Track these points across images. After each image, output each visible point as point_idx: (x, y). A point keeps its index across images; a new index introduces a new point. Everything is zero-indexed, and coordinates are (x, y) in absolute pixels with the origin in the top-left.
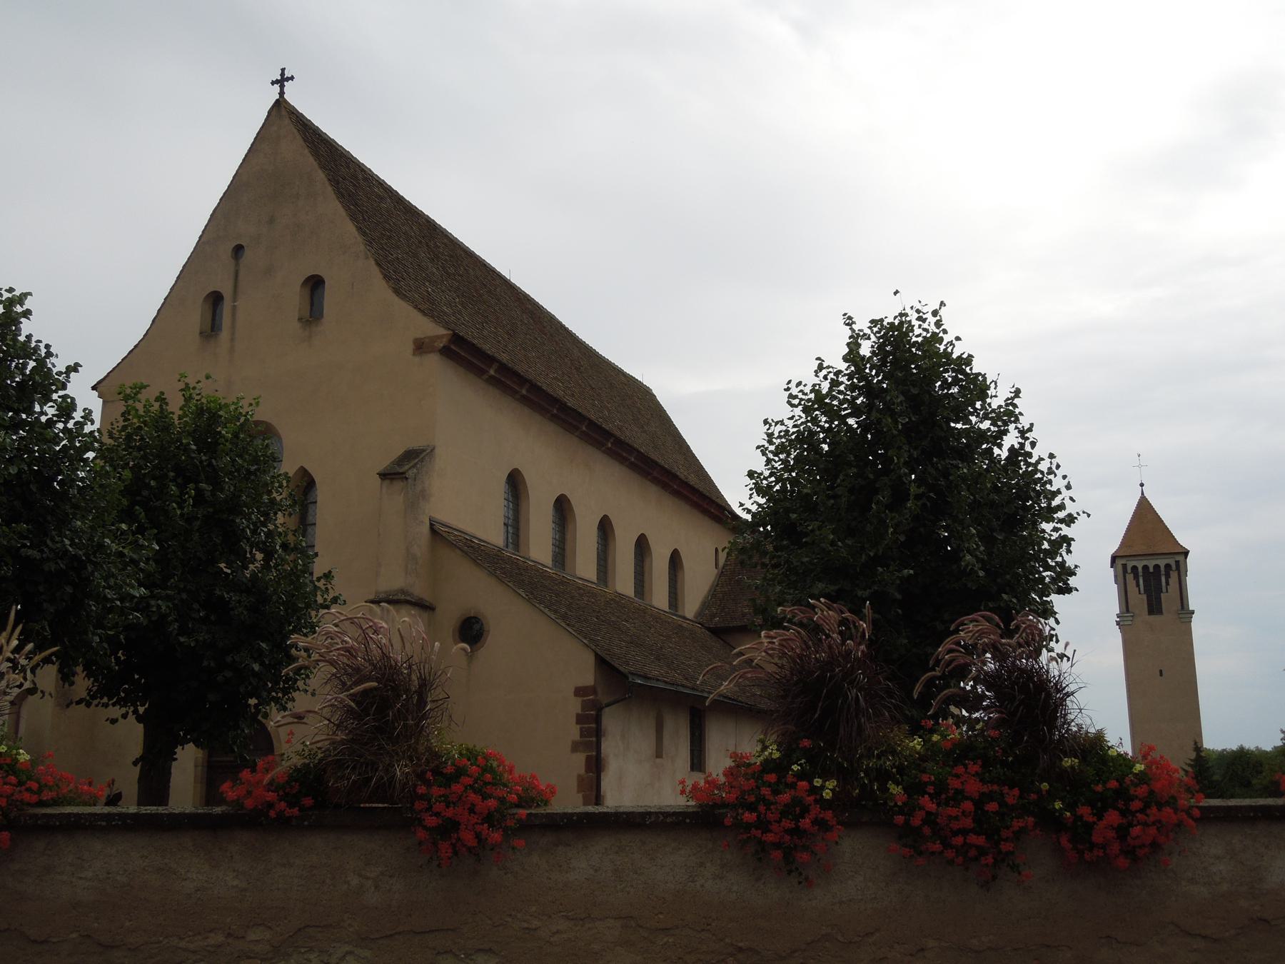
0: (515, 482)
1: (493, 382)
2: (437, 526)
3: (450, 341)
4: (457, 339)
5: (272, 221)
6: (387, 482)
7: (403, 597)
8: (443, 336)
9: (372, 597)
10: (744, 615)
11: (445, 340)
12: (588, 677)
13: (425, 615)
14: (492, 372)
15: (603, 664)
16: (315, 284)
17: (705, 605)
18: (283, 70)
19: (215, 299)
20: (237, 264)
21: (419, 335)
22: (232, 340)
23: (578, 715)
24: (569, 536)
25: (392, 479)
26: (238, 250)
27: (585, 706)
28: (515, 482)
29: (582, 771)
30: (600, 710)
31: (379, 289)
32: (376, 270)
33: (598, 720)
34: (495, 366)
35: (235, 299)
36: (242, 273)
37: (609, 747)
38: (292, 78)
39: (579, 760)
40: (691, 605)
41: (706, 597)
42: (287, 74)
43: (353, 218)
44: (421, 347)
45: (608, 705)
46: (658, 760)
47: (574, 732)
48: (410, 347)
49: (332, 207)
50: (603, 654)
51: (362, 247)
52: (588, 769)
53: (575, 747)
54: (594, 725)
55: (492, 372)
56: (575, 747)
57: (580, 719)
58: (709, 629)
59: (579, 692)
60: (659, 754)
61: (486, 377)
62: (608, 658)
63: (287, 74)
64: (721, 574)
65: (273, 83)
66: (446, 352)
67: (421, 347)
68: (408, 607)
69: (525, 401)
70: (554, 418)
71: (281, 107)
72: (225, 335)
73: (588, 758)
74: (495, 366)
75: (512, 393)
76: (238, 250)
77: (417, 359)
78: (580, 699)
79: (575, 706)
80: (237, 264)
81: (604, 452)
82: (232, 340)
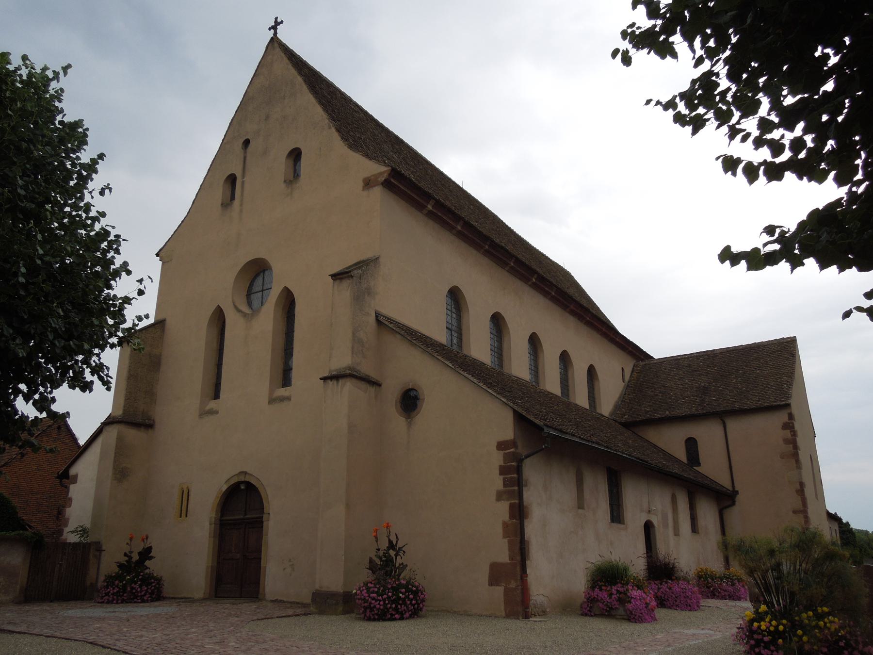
0: (455, 295)
1: (431, 215)
2: (380, 318)
4: (395, 173)
5: (267, 117)
6: (338, 281)
7: (348, 372)
8: (384, 172)
9: (326, 375)
10: (647, 412)
11: (386, 175)
12: (506, 430)
13: (372, 390)
14: (430, 207)
15: (520, 419)
16: (295, 155)
17: (617, 407)
18: (276, 18)
19: (232, 180)
21: (367, 174)
22: (241, 205)
23: (500, 466)
24: (505, 346)
25: (341, 279)
26: (247, 143)
27: (507, 458)
28: (455, 295)
29: (506, 517)
30: (520, 461)
31: (339, 147)
32: (336, 135)
33: (519, 470)
34: (432, 202)
35: (243, 177)
36: (248, 158)
37: (530, 496)
38: (282, 22)
39: (503, 509)
40: (606, 408)
41: (617, 402)
42: (279, 20)
43: (320, 103)
44: (368, 184)
45: (527, 457)
46: (580, 511)
47: (498, 483)
48: (361, 184)
49: (307, 98)
50: (520, 410)
51: (327, 121)
52: (512, 516)
53: (500, 496)
54: (515, 475)
55: (430, 207)
56: (500, 496)
57: (503, 471)
58: (620, 423)
59: (501, 446)
60: (580, 505)
61: (425, 211)
62: (524, 413)
63: (279, 20)
64: (628, 386)
65: (270, 29)
66: (387, 184)
67: (368, 184)
68: (354, 380)
69: (460, 235)
70: (487, 254)
71: (275, 41)
72: (237, 202)
73: (512, 506)
75: (450, 228)
76: (247, 143)
77: (365, 193)
78: (502, 452)
79: (497, 459)
80: (245, 152)
81: (530, 286)
82: (241, 205)
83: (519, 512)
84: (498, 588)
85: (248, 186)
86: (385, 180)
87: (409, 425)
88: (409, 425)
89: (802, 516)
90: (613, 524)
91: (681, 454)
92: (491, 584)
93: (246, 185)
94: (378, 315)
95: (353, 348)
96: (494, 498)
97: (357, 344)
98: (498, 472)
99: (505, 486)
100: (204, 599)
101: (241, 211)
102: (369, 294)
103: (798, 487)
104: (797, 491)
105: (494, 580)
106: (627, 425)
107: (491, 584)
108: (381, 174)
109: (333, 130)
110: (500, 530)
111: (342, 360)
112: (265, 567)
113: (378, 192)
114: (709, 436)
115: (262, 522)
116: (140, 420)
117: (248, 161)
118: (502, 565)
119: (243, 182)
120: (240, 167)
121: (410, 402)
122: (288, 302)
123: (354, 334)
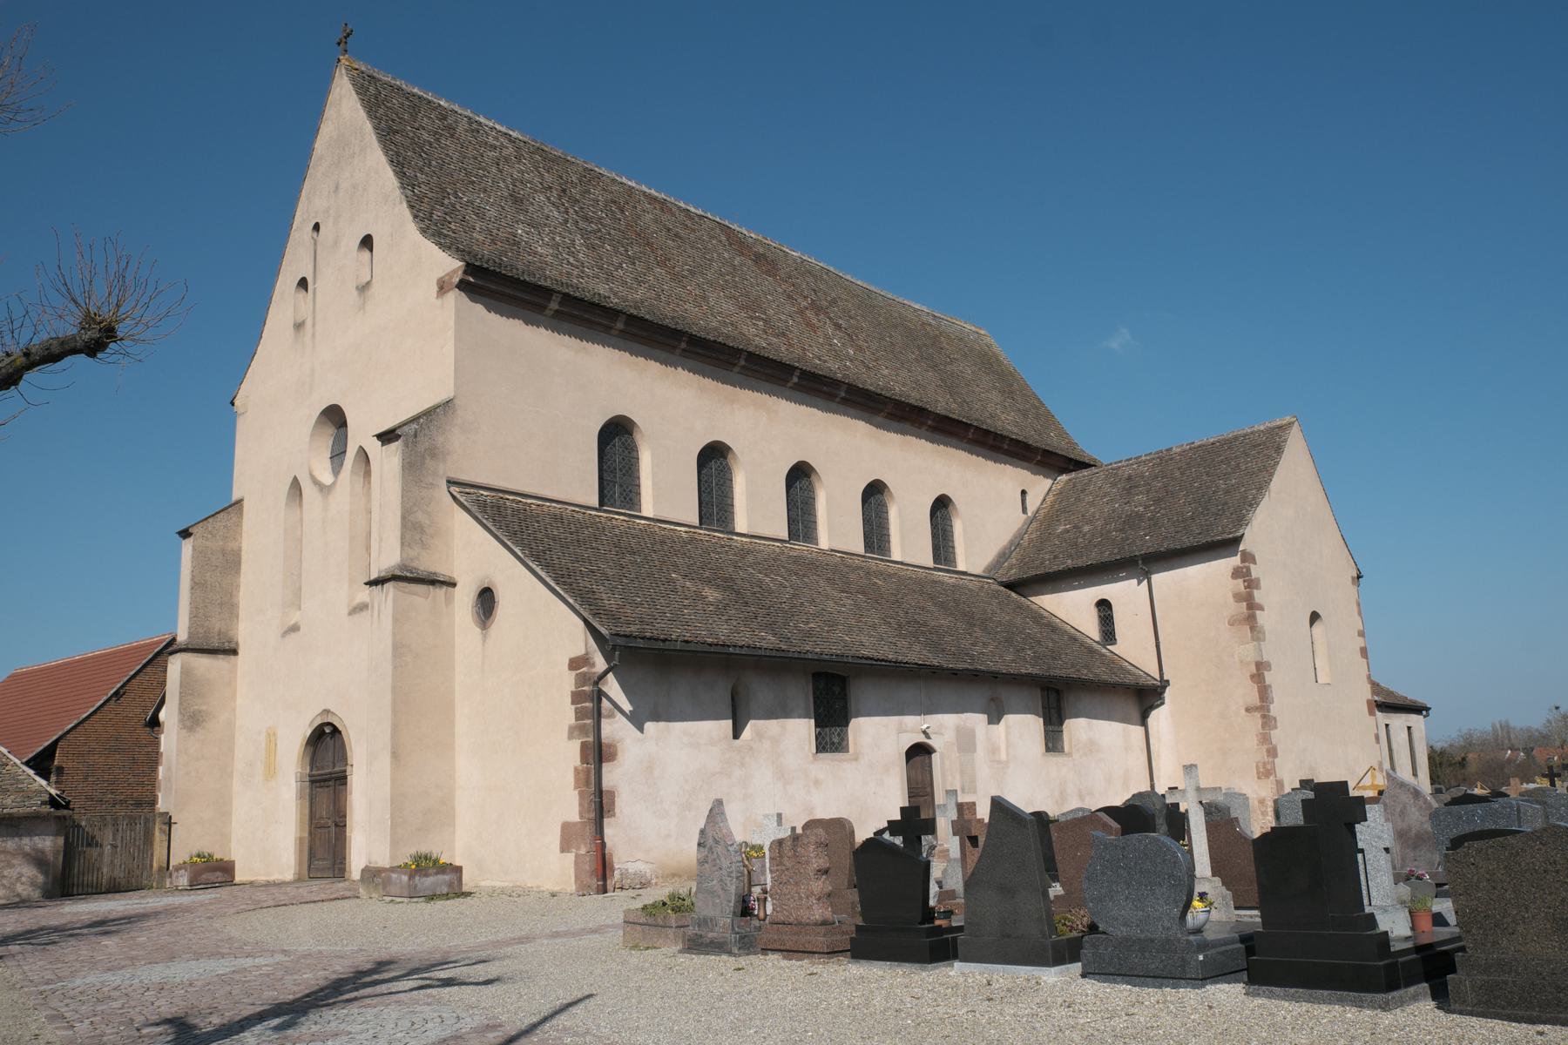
3: (465, 272)
4: (470, 268)
13: (441, 592)
26: (317, 227)
29: (578, 762)
39: (571, 753)
47: (568, 714)
48: (435, 288)
52: (584, 759)
57: (577, 697)
59: (575, 664)
66: (463, 286)
73: (584, 746)
74: (556, 299)
76: (317, 227)
77: (439, 302)
79: (568, 682)
83: (597, 754)
86: (461, 281)
87: (485, 637)
88: (485, 637)
89: (1258, 715)
90: (821, 755)
91: (1090, 627)
92: (562, 851)
94: (451, 482)
95: (403, 537)
96: (566, 735)
97: (413, 528)
99: (577, 719)
100: (295, 881)
102: (433, 456)
103: (1254, 670)
104: (1252, 677)
106: (1010, 586)
107: (562, 851)
108: (455, 271)
109: (405, 204)
110: (570, 778)
111: (388, 557)
113: (454, 297)
114: (1125, 593)
115: (345, 777)
116: (216, 645)
118: (574, 824)
120: (311, 267)
123: (404, 518)
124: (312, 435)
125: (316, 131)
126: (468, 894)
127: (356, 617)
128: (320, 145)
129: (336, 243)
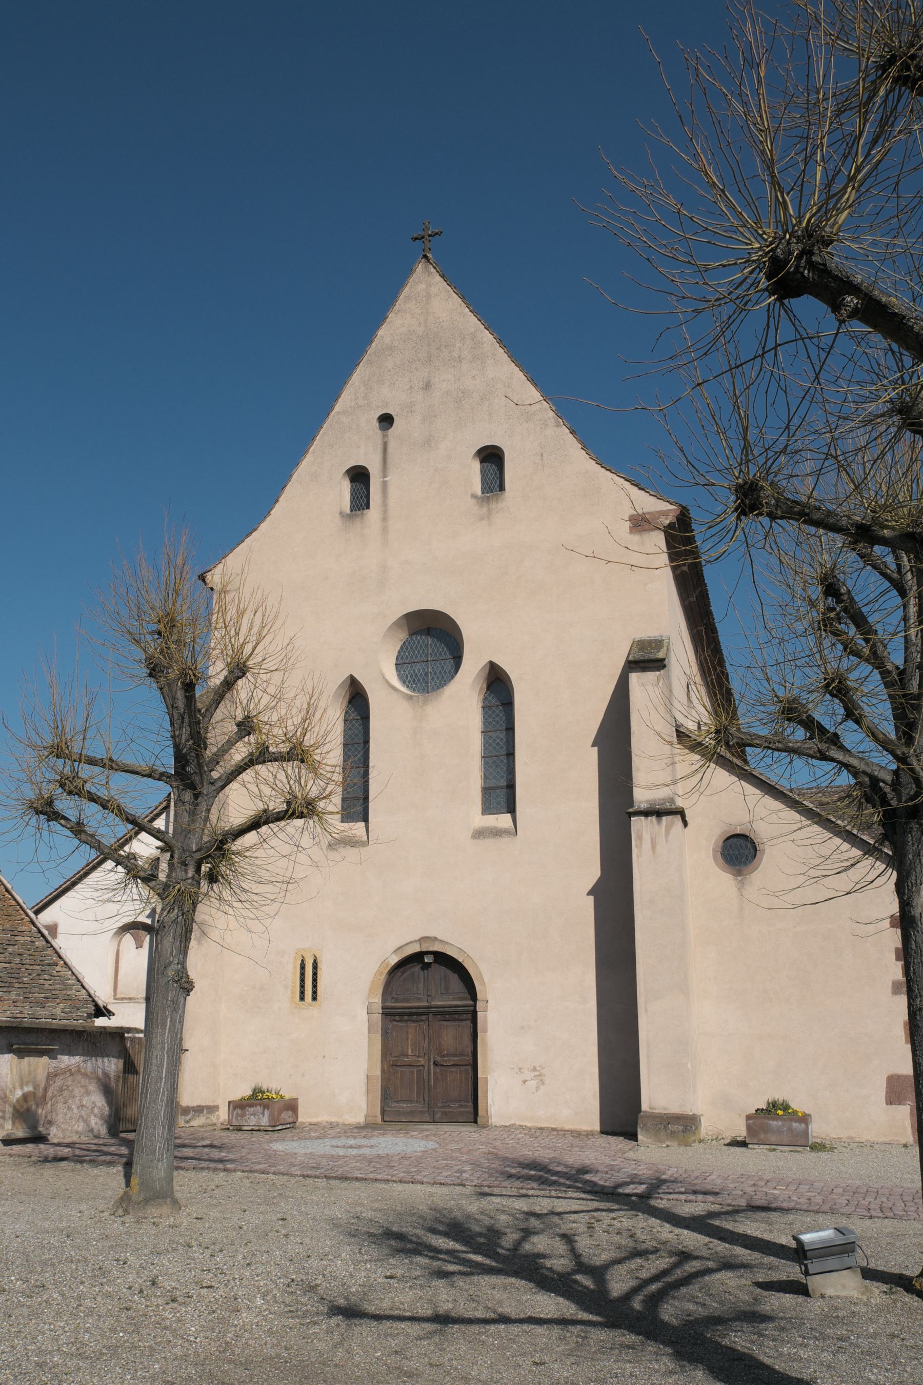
16: (491, 457)
20: (385, 436)
22: (385, 519)
26: (386, 420)
51: (552, 414)
72: (374, 513)
76: (386, 420)
80: (385, 436)
82: (385, 519)
84: (901, 1107)
85: (394, 488)
87: (741, 887)
92: (890, 1102)
93: (392, 491)
96: (889, 990)
98: (894, 956)
100: (368, 1127)
101: (385, 530)
105: (893, 1097)
107: (890, 1102)
112: (486, 1080)
117: (390, 450)
119: (385, 485)
121: (739, 851)
122: (497, 684)
124: (385, 635)
125: (381, 319)
126: (819, 1147)
127: (489, 843)
128: (384, 333)
129: (429, 442)
